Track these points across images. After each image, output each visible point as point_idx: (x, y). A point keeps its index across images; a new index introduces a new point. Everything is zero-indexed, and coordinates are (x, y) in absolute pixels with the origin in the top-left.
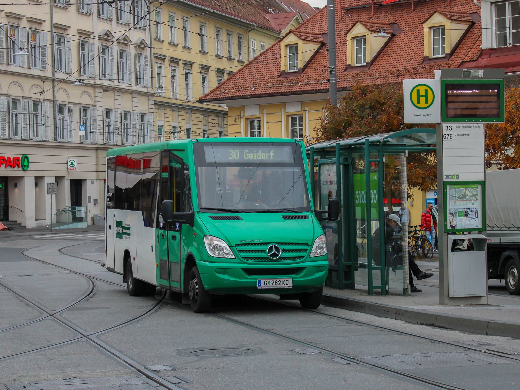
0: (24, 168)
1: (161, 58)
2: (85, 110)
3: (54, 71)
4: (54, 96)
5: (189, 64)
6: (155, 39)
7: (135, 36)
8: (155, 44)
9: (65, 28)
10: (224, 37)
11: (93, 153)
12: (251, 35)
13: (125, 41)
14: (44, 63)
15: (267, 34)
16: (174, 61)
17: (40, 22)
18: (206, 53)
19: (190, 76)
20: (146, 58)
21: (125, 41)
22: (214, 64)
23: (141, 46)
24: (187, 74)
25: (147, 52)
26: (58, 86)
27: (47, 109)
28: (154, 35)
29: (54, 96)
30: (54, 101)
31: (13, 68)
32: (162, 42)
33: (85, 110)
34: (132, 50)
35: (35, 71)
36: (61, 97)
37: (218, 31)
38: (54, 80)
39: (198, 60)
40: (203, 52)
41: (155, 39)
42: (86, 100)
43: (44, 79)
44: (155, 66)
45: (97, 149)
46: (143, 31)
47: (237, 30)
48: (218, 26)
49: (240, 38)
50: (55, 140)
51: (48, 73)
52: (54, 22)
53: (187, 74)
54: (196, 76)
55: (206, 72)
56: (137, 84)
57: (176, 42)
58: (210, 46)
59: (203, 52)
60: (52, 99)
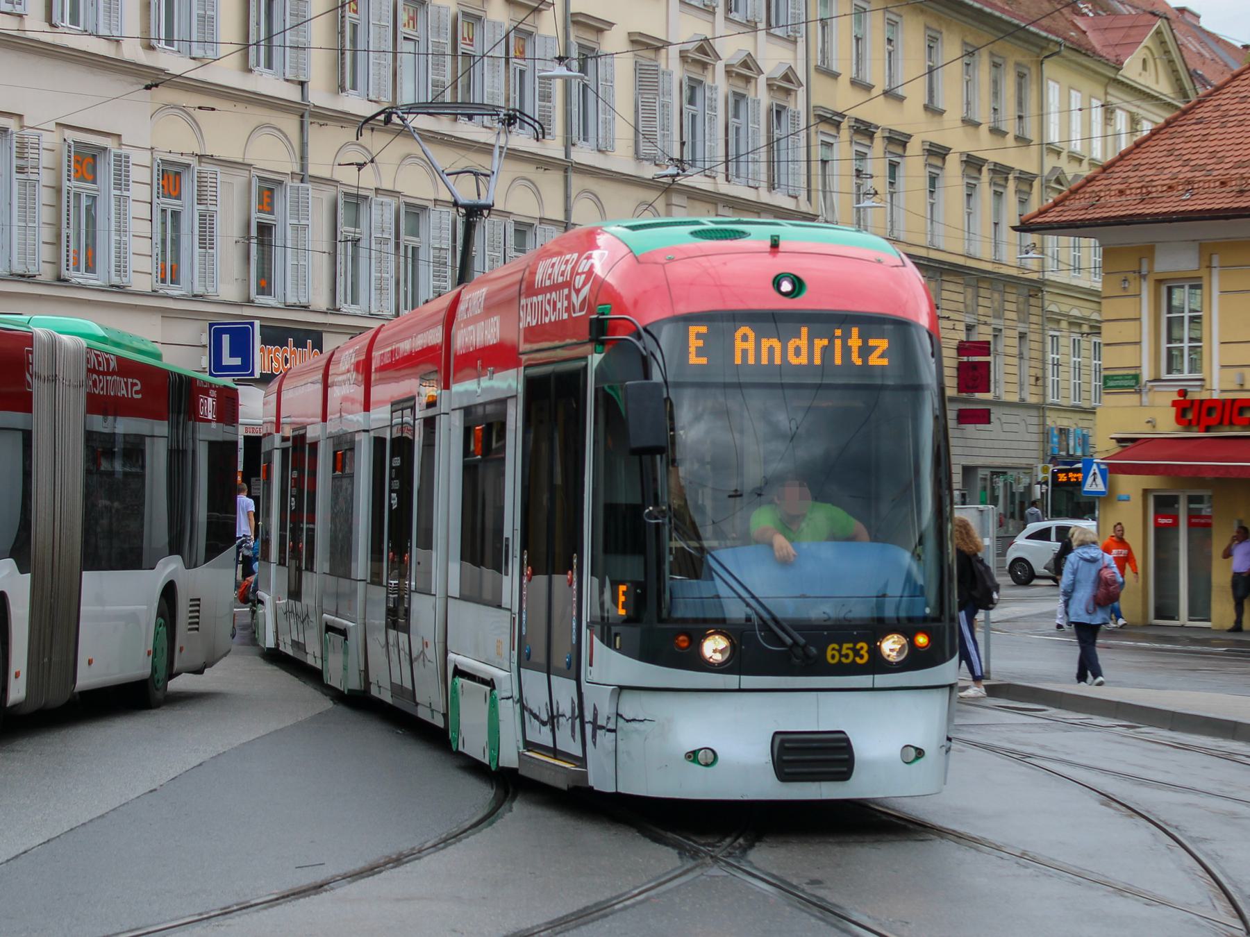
1: (831, 120)
3: (569, 144)
4: (567, 211)
5: (898, 140)
6: (817, 69)
7: (774, 58)
8: (818, 82)
10: (983, 72)
12: (1049, 68)
13: (745, 70)
15: (1087, 68)
16: (864, 130)
18: (941, 113)
19: (901, 172)
20: (795, 117)
21: (745, 70)
22: (959, 141)
23: (785, 84)
24: (893, 166)
25: (798, 104)
26: (577, 182)
28: (816, 59)
29: (567, 211)
32: (835, 76)
34: (761, 96)
37: (970, 53)
38: (567, 168)
39: (922, 130)
40: (932, 109)
41: (817, 69)
44: (816, 140)
46: (791, 46)
47: (1015, 55)
48: (968, 40)
49: (1021, 76)
51: (553, 147)
52: (573, 9)
53: (893, 166)
55: (939, 163)
56: (772, 187)
57: (869, 80)
58: (950, 96)
59: (932, 109)
60: (560, 216)
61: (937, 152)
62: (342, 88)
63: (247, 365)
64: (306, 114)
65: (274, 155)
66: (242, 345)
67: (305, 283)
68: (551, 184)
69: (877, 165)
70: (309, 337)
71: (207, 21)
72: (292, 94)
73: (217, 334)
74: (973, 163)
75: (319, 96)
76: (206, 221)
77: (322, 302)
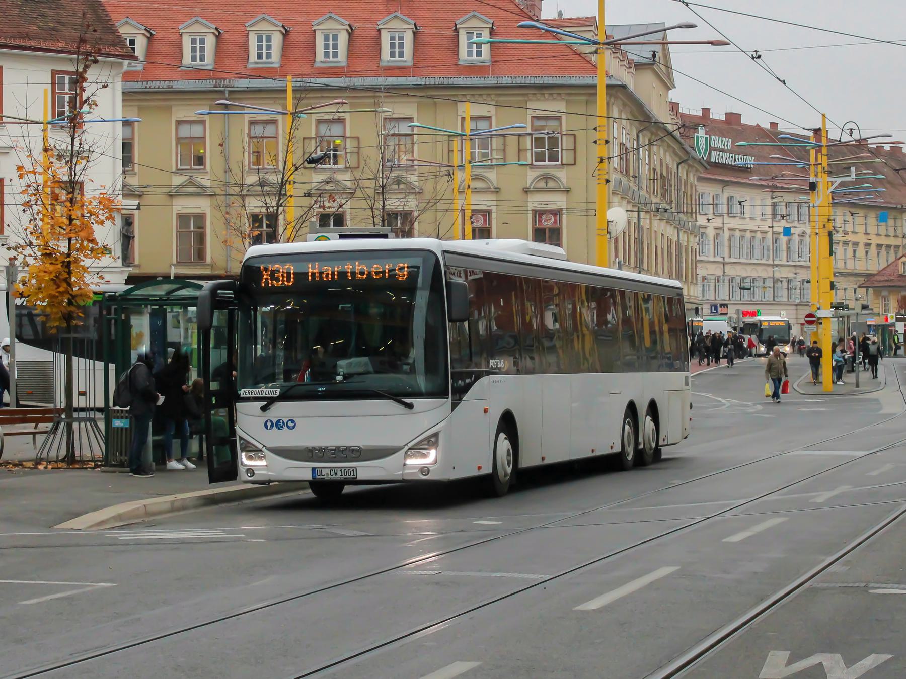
2: (789, 281)
5: (856, 244)
11: (794, 307)
14: (769, 256)
24: (854, 251)
27: (769, 283)
30: (773, 278)
35: (764, 261)
36: (777, 275)
45: (797, 305)
49: (895, 219)
51: (771, 262)
53: (854, 251)
54: (861, 251)
59: (866, 234)
64: (724, 264)
65: (719, 272)
66: (716, 308)
67: (724, 296)
68: (770, 269)
69: (850, 249)
70: (725, 306)
71: (709, 250)
72: (721, 260)
74: (879, 246)
75: (727, 260)
76: (709, 286)
77: (727, 298)
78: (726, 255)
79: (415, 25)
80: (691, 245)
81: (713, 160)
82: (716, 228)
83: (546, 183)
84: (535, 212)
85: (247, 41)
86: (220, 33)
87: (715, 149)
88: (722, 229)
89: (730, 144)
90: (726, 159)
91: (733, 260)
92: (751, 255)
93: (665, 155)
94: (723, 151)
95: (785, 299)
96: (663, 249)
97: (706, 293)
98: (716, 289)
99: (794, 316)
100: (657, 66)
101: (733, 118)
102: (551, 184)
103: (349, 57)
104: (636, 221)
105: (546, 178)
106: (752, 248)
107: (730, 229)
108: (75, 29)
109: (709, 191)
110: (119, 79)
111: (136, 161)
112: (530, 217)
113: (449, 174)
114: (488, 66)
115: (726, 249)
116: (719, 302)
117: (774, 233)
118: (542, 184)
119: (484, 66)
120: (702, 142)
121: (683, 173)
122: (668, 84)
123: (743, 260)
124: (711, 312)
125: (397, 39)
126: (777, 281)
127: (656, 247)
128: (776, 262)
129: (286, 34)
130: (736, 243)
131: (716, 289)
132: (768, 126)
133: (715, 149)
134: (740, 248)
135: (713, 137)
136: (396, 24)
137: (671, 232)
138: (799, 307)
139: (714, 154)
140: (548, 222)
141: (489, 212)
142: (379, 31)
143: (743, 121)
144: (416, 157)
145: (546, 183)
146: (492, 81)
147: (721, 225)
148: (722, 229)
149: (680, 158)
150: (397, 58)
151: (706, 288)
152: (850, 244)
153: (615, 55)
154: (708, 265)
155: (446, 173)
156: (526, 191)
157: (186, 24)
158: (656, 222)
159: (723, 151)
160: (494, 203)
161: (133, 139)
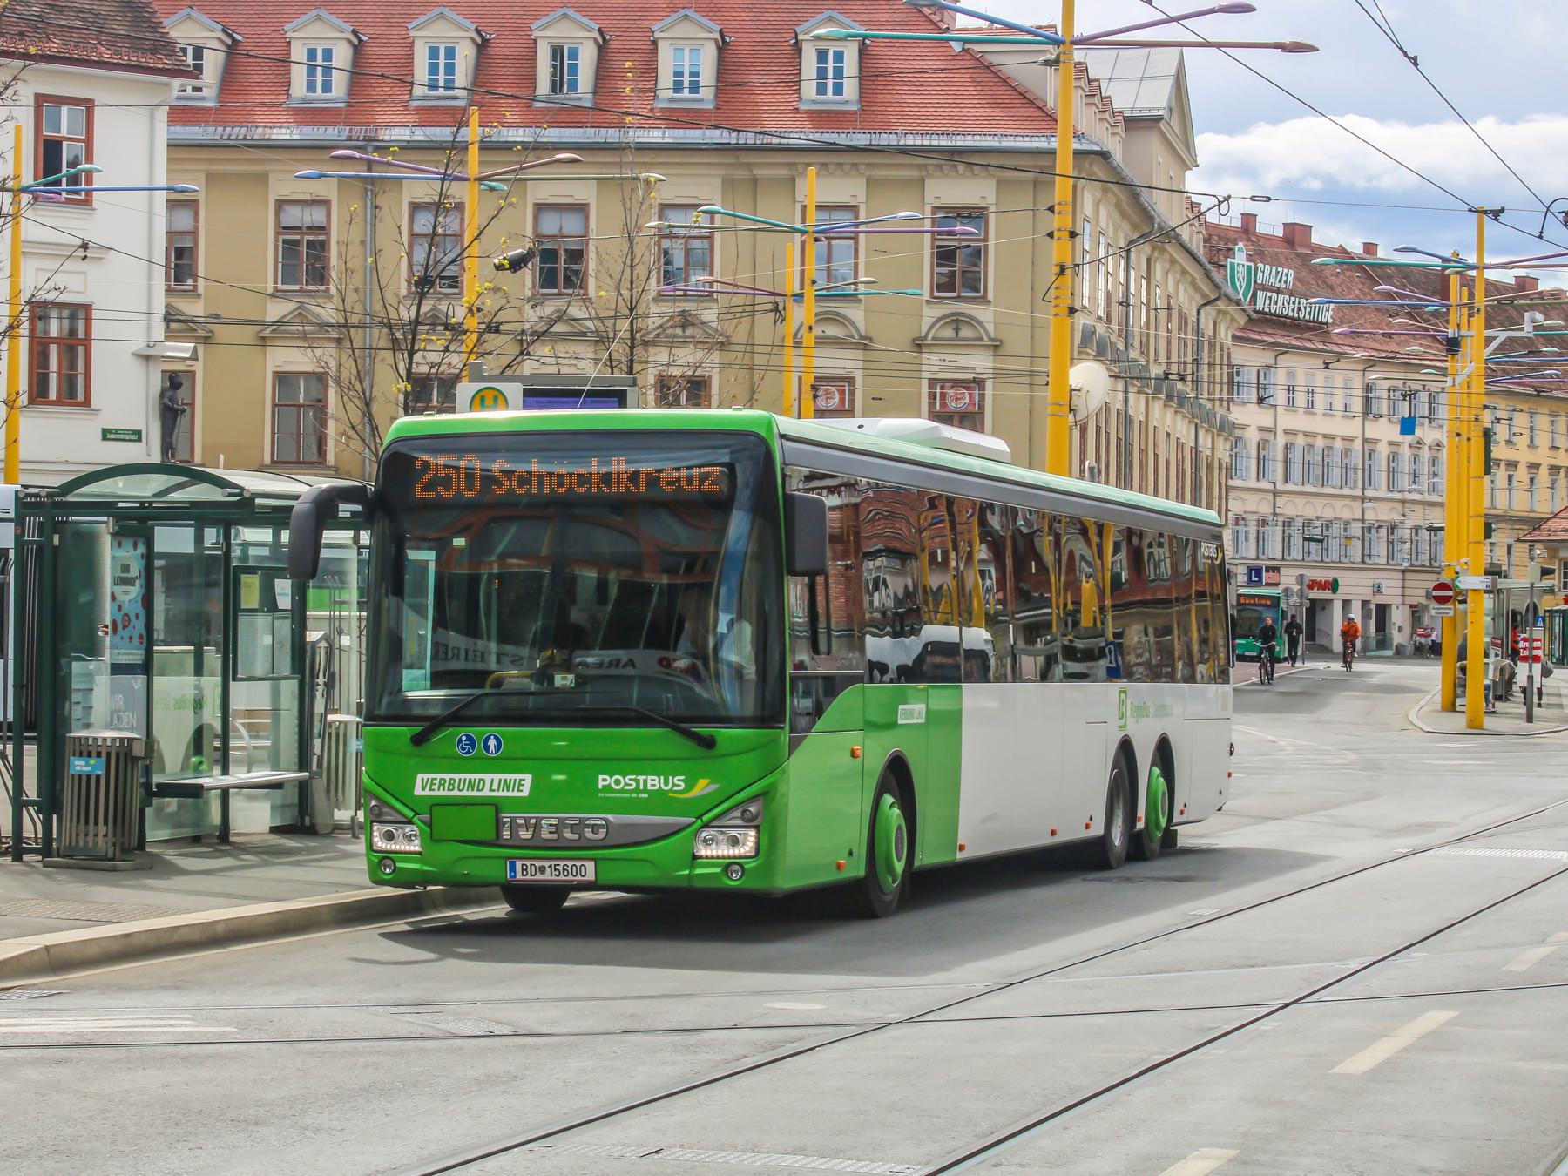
0: (1335, 590)
2: (1393, 528)
9: (1375, 442)
14: (1355, 482)
17: (1351, 439)
24: (1510, 477)
26: (1367, 505)
27: (1356, 529)
30: (1363, 521)
31: (1328, 490)
33: (1393, 528)
35: (1346, 491)
36: (1370, 516)
42: (1397, 517)
43: (1354, 498)
45: (1404, 571)
50: (1363, 562)
51: (1358, 492)
53: (1510, 477)
61: (1534, 466)
62: (1286, 481)
63: (1260, 580)
65: (1266, 509)
66: (1258, 572)
67: (1274, 549)
70: (1276, 569)
71: (1248, 468)
72: (1271, 486)
73: (1250, 570)
75: (1280, 486)
77: (1279, 556)
78: (1279, 477)
79: (721, 32)
80: (1218, 455)
81: (1259, 306)
82: (1261, 429)
83: (957, 330)
84: (932, 382)
85: (410, 58)
86: (360, 41)
87: (1265, 288)
88: (1272, 431)
89: (1290, 279)
90: (1282, 306)
91: (1290, 487)
92: (1325, 481)
93: (1177, 284)
94: (1278, 291)
95: (1383, 561)
96: (1167, 462)
97: (1242, 546)
98: (1260, 539)
99: (1399, 591)
100: (1169, 127)
101: (1295, 236)
102: (966, 332)
103: (596, 92)
104: (1120, 405)
105: (957, 321)
106: (1326, 466)
107: (1286, 432)
108: (83, 19)
109: (1249, 359)
110: (162, 115)
111: (201, 272)
112: (925, 390)
113: (776, 310)
114: (855, 113)
115: (1280, 467)
116: (1263, 563)
117: (1365, 441)
118: (949, 333)
119: (845, 113)
120: (1241, 274)
121: (1207, 326)
122: (1185, 158)
123: (1308, 488)
124: (1250, 580)
125: (686, 56)
126: (1368, 529)
127: (1156, 455)
128: (1369, 493)
129: (483, 47)
130: (1297, 456)
131: (1260, 539)
132: (1360, 250)
133: (1265, 288)
134: (1307, 465)
135: (1260, 266)
136: (686, 30)
137: (1182, 429)
138: (1408, 576)
139: (1261, 296)
140: (960, 401)
141: (850, 380)
142: (655, 43)
143: (1315, 239)
144: (717, 276)
145: (957, 330)
146: (861, 139)
147: (1271, 425)
148: (1272, 431)
149: (1204, 296)
150: (686, 94)
151: (1242, 537)
152: (1502, 465)
153: (1091, 100)
154: (1244, 495)
155: (771, 307)
156: (919, 345)
157: (296, 22)
158: (1157, 407)
159: (1278, 291)
160: (860, 365)
161: (194, 233)
